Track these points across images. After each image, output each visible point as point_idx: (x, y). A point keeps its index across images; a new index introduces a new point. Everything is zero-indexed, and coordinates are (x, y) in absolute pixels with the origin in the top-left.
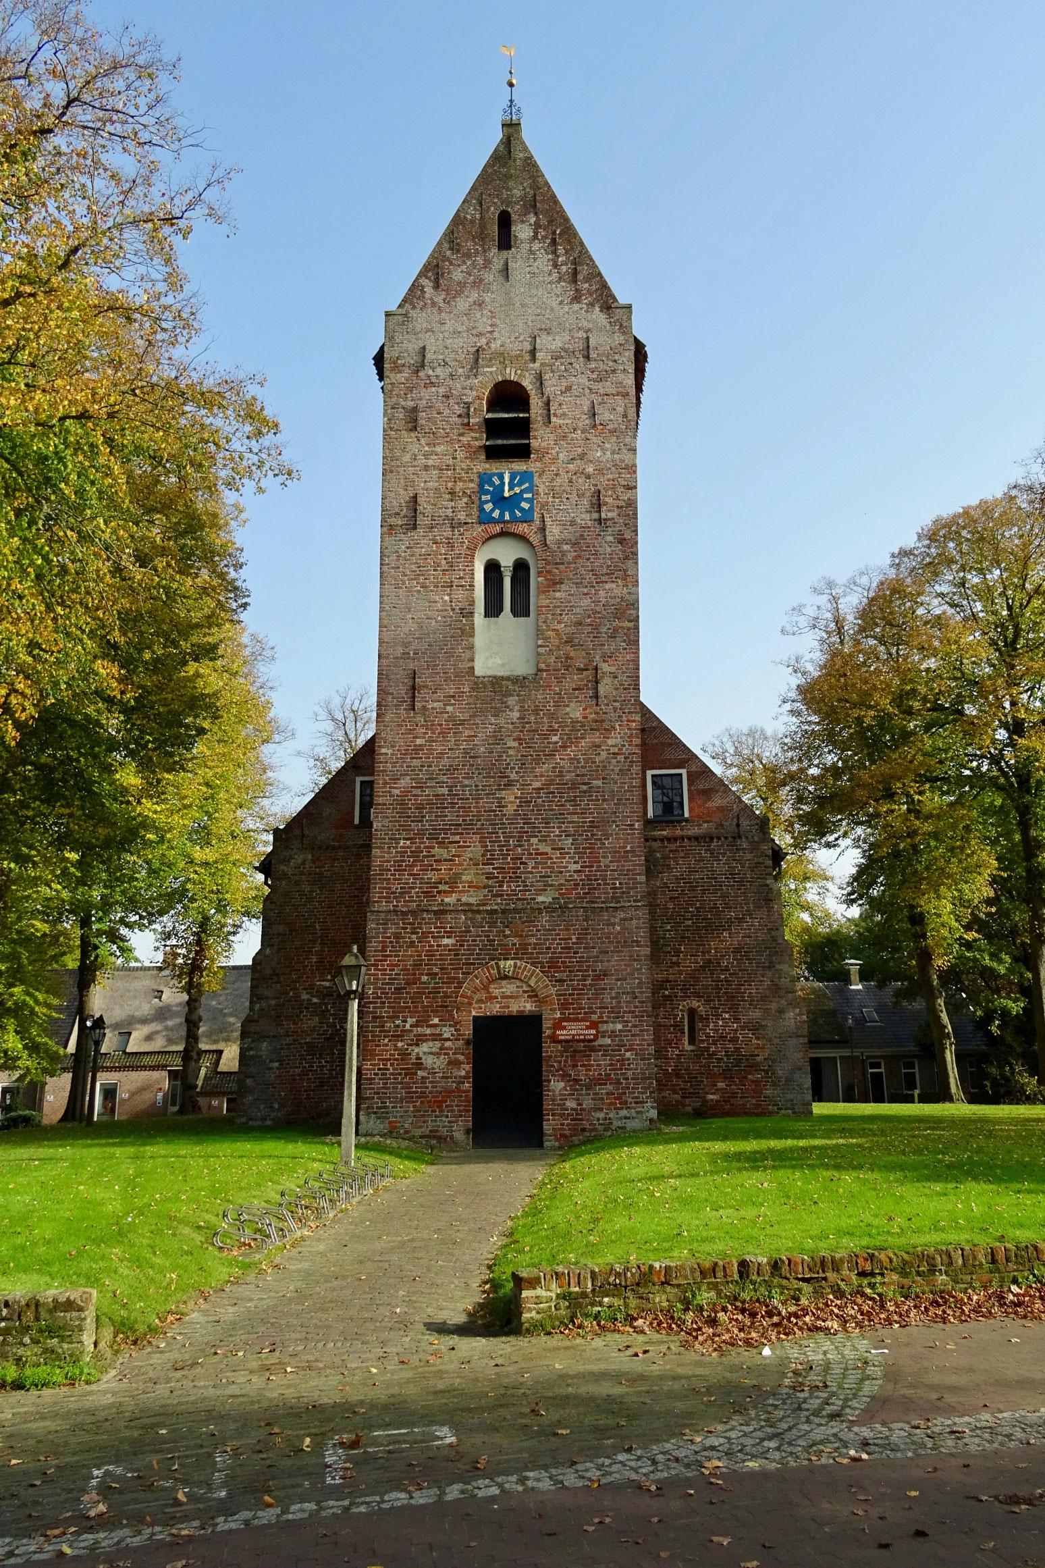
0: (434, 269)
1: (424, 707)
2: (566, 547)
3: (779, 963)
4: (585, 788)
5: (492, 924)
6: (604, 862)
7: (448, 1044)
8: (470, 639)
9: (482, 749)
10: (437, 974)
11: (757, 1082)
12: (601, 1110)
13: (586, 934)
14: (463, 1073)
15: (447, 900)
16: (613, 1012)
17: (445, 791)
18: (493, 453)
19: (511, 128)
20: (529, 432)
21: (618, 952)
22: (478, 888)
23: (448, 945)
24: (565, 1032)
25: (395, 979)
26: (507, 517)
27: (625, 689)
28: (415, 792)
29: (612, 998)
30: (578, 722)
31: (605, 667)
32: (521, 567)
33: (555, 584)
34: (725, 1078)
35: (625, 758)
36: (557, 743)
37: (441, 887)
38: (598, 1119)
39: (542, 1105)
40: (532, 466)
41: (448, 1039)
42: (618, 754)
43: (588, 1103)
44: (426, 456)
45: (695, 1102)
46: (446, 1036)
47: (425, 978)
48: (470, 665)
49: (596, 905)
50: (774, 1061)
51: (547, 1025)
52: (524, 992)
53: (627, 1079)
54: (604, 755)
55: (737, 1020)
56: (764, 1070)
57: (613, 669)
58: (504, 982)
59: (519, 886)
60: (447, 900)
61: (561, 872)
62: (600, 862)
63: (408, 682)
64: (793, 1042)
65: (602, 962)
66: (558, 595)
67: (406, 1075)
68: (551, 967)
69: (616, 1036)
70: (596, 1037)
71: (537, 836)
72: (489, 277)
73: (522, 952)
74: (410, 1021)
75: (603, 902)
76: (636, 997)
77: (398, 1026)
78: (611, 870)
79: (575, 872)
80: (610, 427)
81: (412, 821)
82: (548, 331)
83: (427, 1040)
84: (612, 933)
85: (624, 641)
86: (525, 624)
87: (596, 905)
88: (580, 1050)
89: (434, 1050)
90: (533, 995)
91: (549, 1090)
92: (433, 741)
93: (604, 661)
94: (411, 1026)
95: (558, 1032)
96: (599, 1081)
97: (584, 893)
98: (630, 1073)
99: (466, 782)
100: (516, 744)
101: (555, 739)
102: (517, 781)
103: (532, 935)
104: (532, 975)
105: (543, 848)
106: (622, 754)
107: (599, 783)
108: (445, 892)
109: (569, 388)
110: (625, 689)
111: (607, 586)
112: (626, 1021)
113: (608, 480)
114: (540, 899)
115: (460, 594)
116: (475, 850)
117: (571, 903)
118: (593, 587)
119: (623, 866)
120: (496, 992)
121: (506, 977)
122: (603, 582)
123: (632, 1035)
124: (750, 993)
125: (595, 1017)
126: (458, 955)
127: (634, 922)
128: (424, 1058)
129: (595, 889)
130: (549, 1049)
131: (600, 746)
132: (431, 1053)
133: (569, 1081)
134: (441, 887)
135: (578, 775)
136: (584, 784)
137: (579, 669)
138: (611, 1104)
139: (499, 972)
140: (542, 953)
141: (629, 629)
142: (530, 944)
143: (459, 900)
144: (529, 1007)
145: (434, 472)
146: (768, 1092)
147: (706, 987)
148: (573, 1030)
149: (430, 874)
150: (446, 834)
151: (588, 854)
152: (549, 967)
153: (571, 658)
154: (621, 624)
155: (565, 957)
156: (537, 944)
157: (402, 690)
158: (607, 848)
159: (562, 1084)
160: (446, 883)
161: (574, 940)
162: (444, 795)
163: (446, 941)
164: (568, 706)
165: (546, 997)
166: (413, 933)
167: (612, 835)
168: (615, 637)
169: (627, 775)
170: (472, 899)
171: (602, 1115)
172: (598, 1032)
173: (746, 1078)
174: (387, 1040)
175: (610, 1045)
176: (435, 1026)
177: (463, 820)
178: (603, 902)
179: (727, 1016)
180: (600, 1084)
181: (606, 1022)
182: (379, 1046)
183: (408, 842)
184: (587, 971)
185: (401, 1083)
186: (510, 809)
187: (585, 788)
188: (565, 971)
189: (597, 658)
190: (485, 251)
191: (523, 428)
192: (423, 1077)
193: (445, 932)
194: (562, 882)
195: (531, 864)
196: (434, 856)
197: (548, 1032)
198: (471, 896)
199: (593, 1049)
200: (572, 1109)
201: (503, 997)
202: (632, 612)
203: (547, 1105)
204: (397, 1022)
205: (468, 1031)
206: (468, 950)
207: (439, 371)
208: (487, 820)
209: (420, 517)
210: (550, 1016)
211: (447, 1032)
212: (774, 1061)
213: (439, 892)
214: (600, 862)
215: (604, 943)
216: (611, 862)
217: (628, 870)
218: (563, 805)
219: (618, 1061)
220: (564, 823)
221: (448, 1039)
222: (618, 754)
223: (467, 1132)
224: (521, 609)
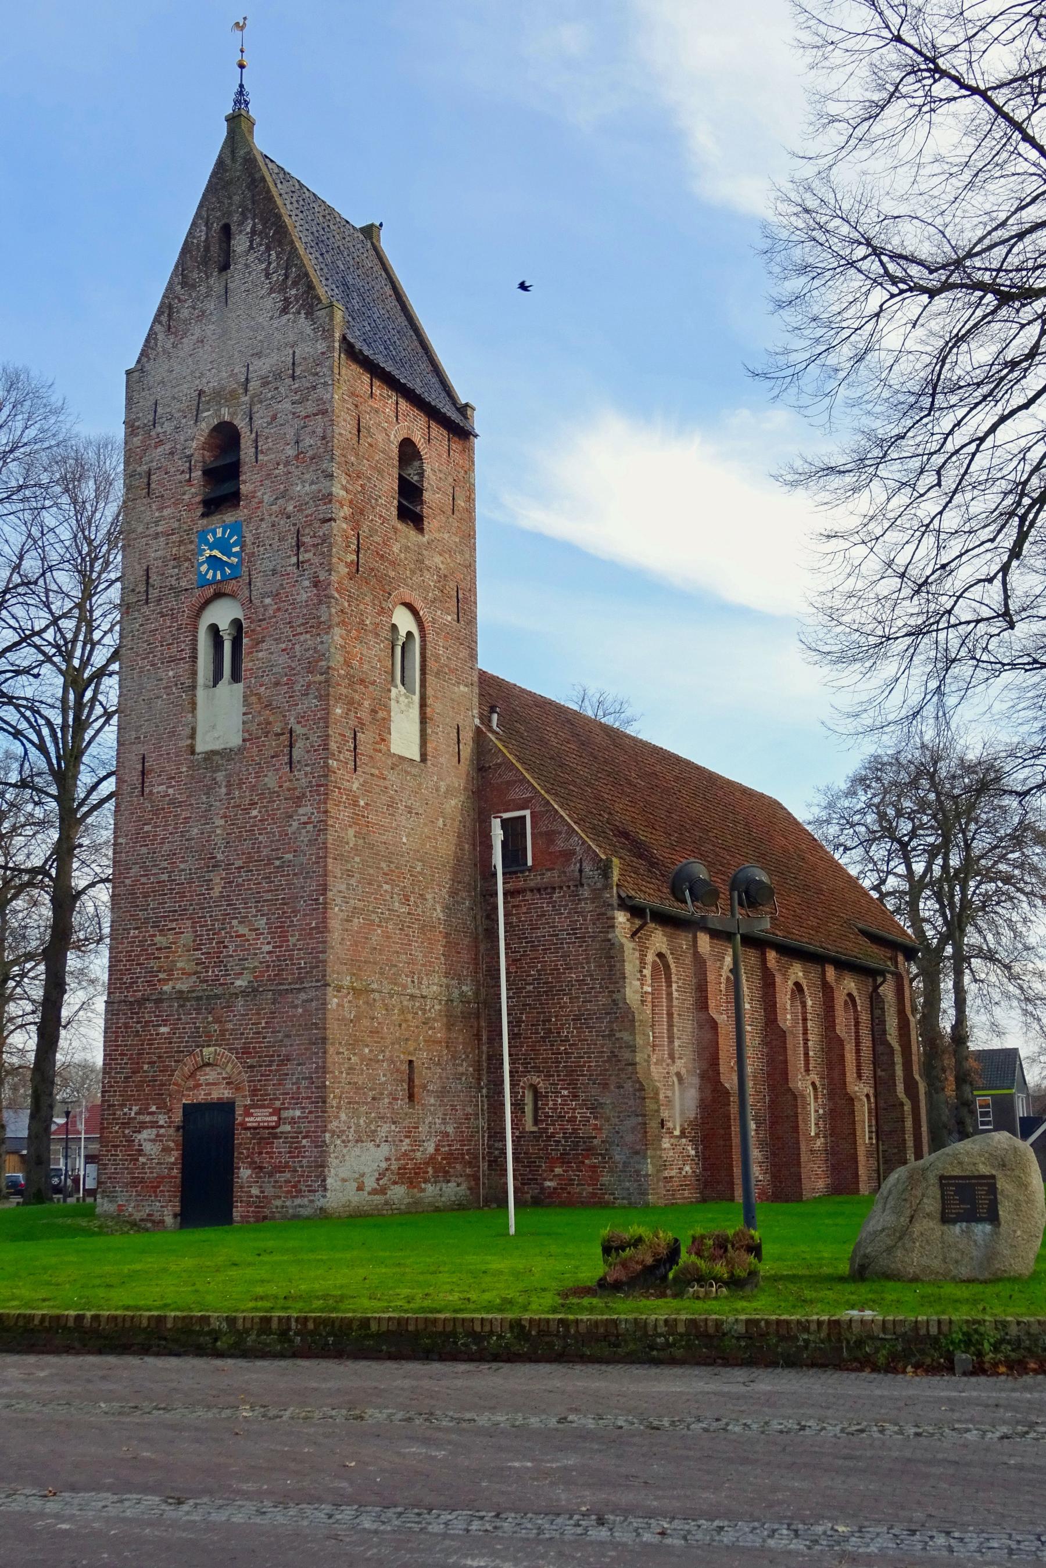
0: (167, 311)
1: (151, 793)
2: (268, 601)
3: (620, 1031)
4: (277, 863)
5: (198, 1010)
6: (292, 940)
7: (162, 1131)
9: (196, 831)
10: (155, 1062)
11: (593, 1168)
13: (273, 1018)
14: (173, 1160)
15: (165, 988)
16: (293, 1098)
17: (165, 877)
20: (239, 476)
21: (299, 1035)
22: (190, 974)
23: (163, 1034)
24: (252, 1119)
25: (124, 1068)
26: (219, 577)
27: (315, 751)
28: (143, 880)
29: (293, 1084)
30: (275, 792)
31: (299, 730)
33: (258, 644)
34: (563, 1163)
35: (314, 827)
36: (256, 817)
37: (161, 976)
38: (277, 1207)
40: (242, 513)
41: (162, 1127)
42: (307, 823)
43: (269, 1191)
44: (157, 523)
45: (533, 1189)
46: (161, 1123)
49: (281, 987)
50: (611, 1144)
51: (239, 1111)
52: (224, 1078)
53: (302, 1167)
54: (295, 824)
55: (575, 1097)
56: (601, 1154)
58: (208, 1069)
59: (221, 971)
60: (165, 988)
61: (256, 954)
62: (288, 941)
63: (139, 767)
65: (286, 1046)
66: (260, 655)
69: (295, 1123)
71: (237, 918)
72: (211, 305)
73: (221, 1040)
74: (135, 1108)
75: (290, 984)
76: (313, 1083)
77: (125, 1114)
78: (299, 949)
79: (269, 953)
80: (310, 453)
81: (140, 910)
82: (258, 355)
83: (147, 1127)
84: (294, 1016)
86: (240, 687)
87: (281, 987)
88: (266, 1136)
89: (153, 1137)
91: (238, 1177)
92: (159, 826)
94: (136, 1114)
95: (247, 1119)
96: (280, 1169)
97: (275, 975)
98: (305, 1160)
99: (182, 866)
100: (222, 822)
101: (254, 813)
102: (222, 861)
103: (230, 1021)
105: (243, 930)
106: (311, 823)
107: (289, 856)
108: (164, 980)
109: (274, 418)
110: (315, 751)
111: (302, 638)
112: (303, 1108)
113: (306, 517)
114: (238, 983)
116: (187, 938)
119: (308, 944)
121: (208, 1065)
123: (309, 1122)
124: (589, 1066)
125: (278, 1104)
126: (170, 1043)
127: (314, 1004)
128: (144, 1144)
129: (283, 970)
130: (241, 1137)
131: (291, 817)
132: (150, 1140)
133: (255, 1168)
134: (161, 976)
135: (273, 850)
136: (278, 859)
137: (278, 735)
138: (288, 1192)
140: (237, 1039)
142: (227, 1030)
143: (174, 988)
144: (226, 1094)
146: (605, 1179)
147: (545, 1060)
148: (261, 1117)
149: (152, 963)
152: (243, 1053)
153: (270, 723)
154: (312, 679)
155: (256, 1043)
156: (233, 1030)
157: (135, 778)
158: (295, 926)
159: (249, 1172)
160: (165, 971)
161: (263, 1025)
162: (164, 881)
163: (163, 1030)
164: (266, 776)
166: (138, 1023)
168: (307, 694)
169: (314, 845)
171: (278, 1203)
172: (280, 1119)
173: (583, 1162)
175: (289, 1132)
177: (180, 906)
179: (565, 1093)
180: (281, 1172)
181: (288, 1109)
182: (111, 1133)
184: (273, 1056)
185: (127, 1169)
186: (216, 892)
187: (277, 863)
188: (254, 1057)
189: (292, 720)
190: (207, 278)
192: (143, 1164)
193: (163, 1021)
194: (256, 964)
196: (155, 944)
197: (239, 1119)
199: (276, 1136)
200: (257, 1197)
201: (207, 1084)
203: (237, 1193)
205: (178, 1117)
206: (179, 1038)
208: (197, 904)
209: (150, 589)
210: (243, 1101)
211: (162, 1120)
212: (611, 1144)
213: (159, 981)
214: (288, 941)
216: (298, 940)
217: (312, 949)
218: (259, 883)
219: (296, 1148)
220: (259, 902)
221: (162, 1127)
222: (307, 823)
223: (175, 1216)
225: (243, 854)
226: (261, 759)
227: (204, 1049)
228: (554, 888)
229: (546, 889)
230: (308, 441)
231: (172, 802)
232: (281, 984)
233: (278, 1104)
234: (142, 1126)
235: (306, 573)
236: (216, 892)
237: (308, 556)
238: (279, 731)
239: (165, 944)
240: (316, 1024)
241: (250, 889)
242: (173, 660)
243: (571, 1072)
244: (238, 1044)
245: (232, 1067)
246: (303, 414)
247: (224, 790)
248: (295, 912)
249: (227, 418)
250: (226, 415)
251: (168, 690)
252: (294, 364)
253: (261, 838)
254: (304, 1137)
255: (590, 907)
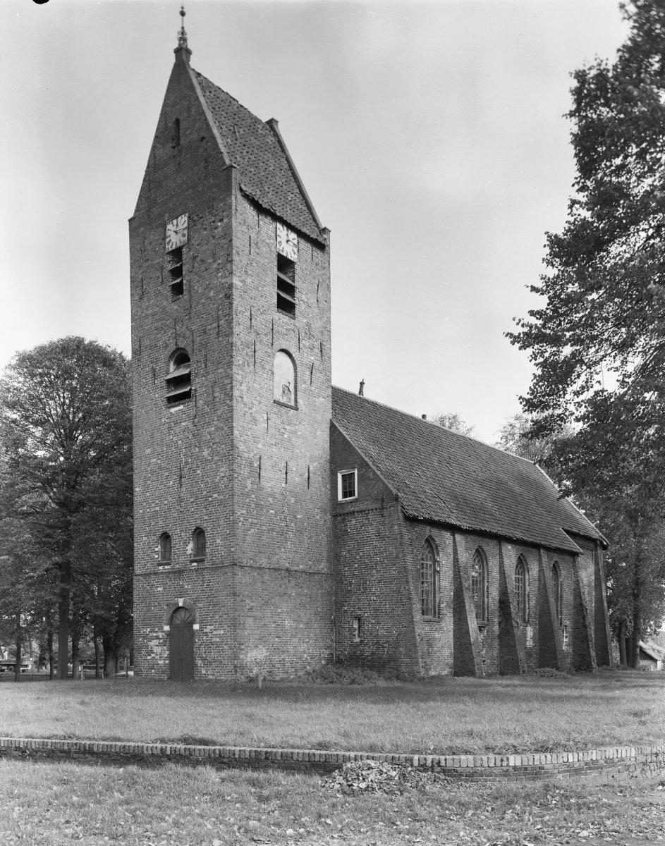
6: (218, 541)
17: (158, 508)
89: (157, 644)
107: (215, 495)
119: (225, 543)
211: (160, 635)
232: (213, 564)
234: (152, 638)
243: (376, 610)
248: (219, 526)
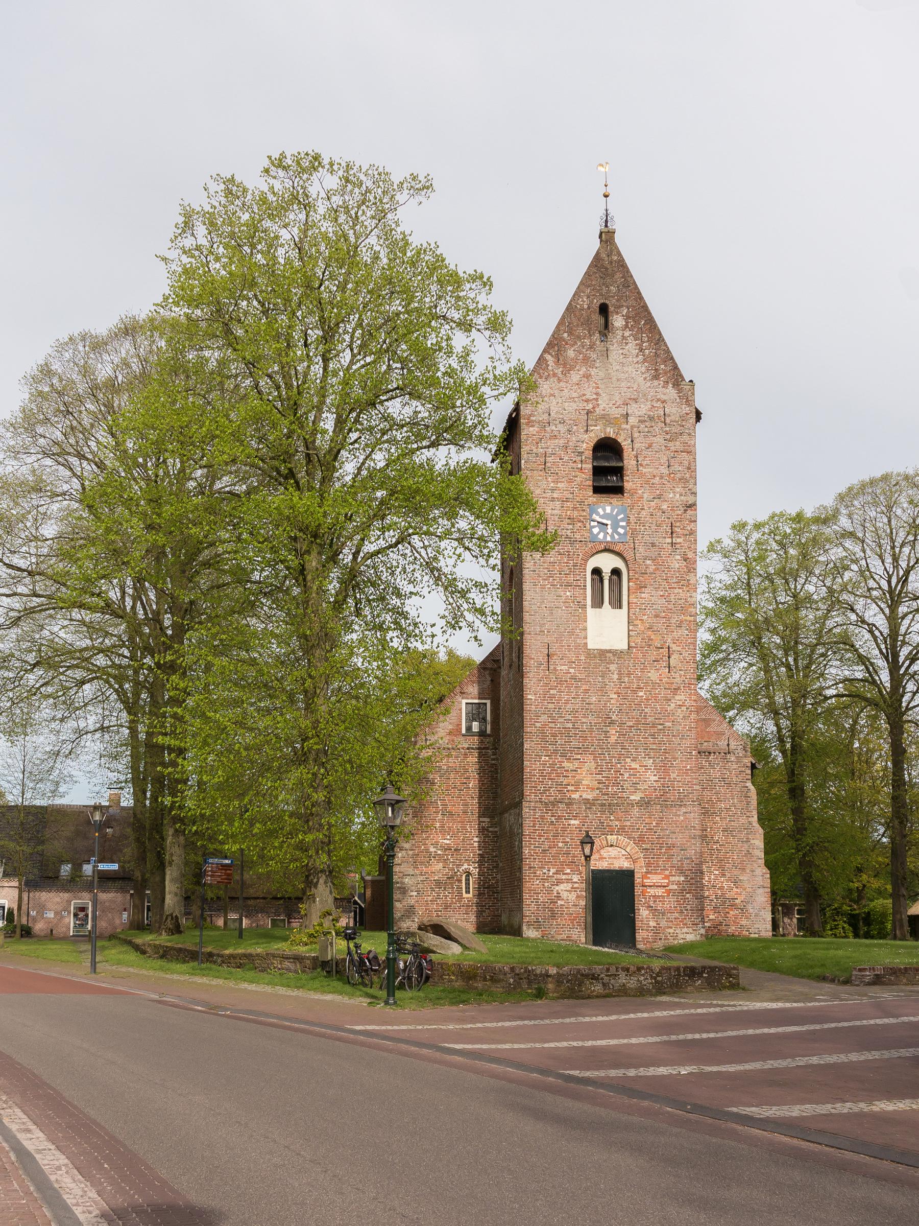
1: (555, 669)
2: (648, 562)
4: (660, 727)
5: (603, 812)
6: (673, 776)
7: (576, 885)
8: (585, 624)
9: (594, 699)
12: (671, 928)
15: (573, 796)
17: (570, 725)
18: (597, 490)
19: (607, 237)
22: (593, 789)
24: (649, 881)
27: (687, 662)
28: (551, 725)
30: (656, 683)
31: (674, 647)
32: (616, 572)
33: (641, 587)
37: (570, 788)
39: (635, 924)
40: (627, 499)
41: (576, 883)
44: (553, 490)
46: (574, 880)
47: (560, 845)
48: (585, 641)
52: (623, 855)
54: (673, 705)
57: (679, 649)
58: (610, 849)
61: (646, 781)
64: (761, 891)
66: (643, 595)
67: (551, 903)
68: (640, 841)
70: (668, 884)
73: (622, 831)
74: (552, 871)
75: (672, 801)
77: (545, 873)
85: (687, 630)
89: (568, 888)
90: (629, 857)
93: (674, 643)
95: (645, 881)
99: (584, 720)
100: (615, 696)
101: (641, 694)
102: (617, 721)
104: (628, 845)
105: (634, 765)
107: (670, 724)
109: (650, 446)
110: (687, 662)
111: (676, 591)
115: (578, 592)
117: (652, 801)
118: (667, 591)
120: (605, 855)
122: (673, 588)
125: (667, 873)
127: (692, 814)
128: (561, 893)
131: (670, 700)
134: (570, 788)
139: (607, 843)
141: (690, 621)
143: (581, 796)
144: (626, 865)
145: (558, 503)
149: (562, 779)
150: (572, 753)
151: (664, 768)
154: (685, 618)
159: (647, 912)
160: (572, 785)
161: (654, 825)
163: (572, 822)
165: (638, 859)
166: (552, 816)
167: (678, 758)
170: (589, 796)
171: (671, 931)
172: (669, 881)
174: (538, 882)
176: (569, 874)
177: (583, 745)
178: (672, 801)
183: (547, 758)
186: (613, 739)
187: (660, 727)
190: (590, 336)
191: (619, 471)
195: (626, 775)
196: (564, 767)
198: (588, 794)
201: (609, 858)
202: (692, 609)
203: (638, 924)
204: (544, 871)
207: (560, 427)
215: (673, 827)
221: (576, 883)
224: (617, 603)
225: (633, 718)
226: (645, 661)
227: (608, 837)
228: (710, 753)
229: (705, 752)
230: (677, 467)
231: (573, 678)
233: (667, 873)
234: (559, 882)
235: (678, 551)
236: (613, 739)
237: (679, 540)
238: (659, 646)
239: (571, 768)
240: (694, 827)
241: (640, 741)
242: (569, 585)
244: (636, 835)
245: (631, 847)
246: (673, 448)
247: (615, 676)
248: (675, 759)
249: (612, 435)
250: (611, 432)
251: (567, 605)
252: (664, 415)
253: (646, 710)
254: (688, 893)
255: (735, 766)
